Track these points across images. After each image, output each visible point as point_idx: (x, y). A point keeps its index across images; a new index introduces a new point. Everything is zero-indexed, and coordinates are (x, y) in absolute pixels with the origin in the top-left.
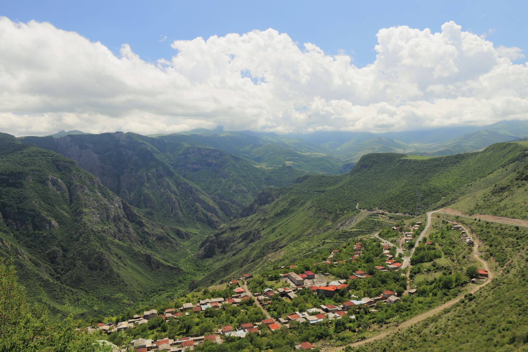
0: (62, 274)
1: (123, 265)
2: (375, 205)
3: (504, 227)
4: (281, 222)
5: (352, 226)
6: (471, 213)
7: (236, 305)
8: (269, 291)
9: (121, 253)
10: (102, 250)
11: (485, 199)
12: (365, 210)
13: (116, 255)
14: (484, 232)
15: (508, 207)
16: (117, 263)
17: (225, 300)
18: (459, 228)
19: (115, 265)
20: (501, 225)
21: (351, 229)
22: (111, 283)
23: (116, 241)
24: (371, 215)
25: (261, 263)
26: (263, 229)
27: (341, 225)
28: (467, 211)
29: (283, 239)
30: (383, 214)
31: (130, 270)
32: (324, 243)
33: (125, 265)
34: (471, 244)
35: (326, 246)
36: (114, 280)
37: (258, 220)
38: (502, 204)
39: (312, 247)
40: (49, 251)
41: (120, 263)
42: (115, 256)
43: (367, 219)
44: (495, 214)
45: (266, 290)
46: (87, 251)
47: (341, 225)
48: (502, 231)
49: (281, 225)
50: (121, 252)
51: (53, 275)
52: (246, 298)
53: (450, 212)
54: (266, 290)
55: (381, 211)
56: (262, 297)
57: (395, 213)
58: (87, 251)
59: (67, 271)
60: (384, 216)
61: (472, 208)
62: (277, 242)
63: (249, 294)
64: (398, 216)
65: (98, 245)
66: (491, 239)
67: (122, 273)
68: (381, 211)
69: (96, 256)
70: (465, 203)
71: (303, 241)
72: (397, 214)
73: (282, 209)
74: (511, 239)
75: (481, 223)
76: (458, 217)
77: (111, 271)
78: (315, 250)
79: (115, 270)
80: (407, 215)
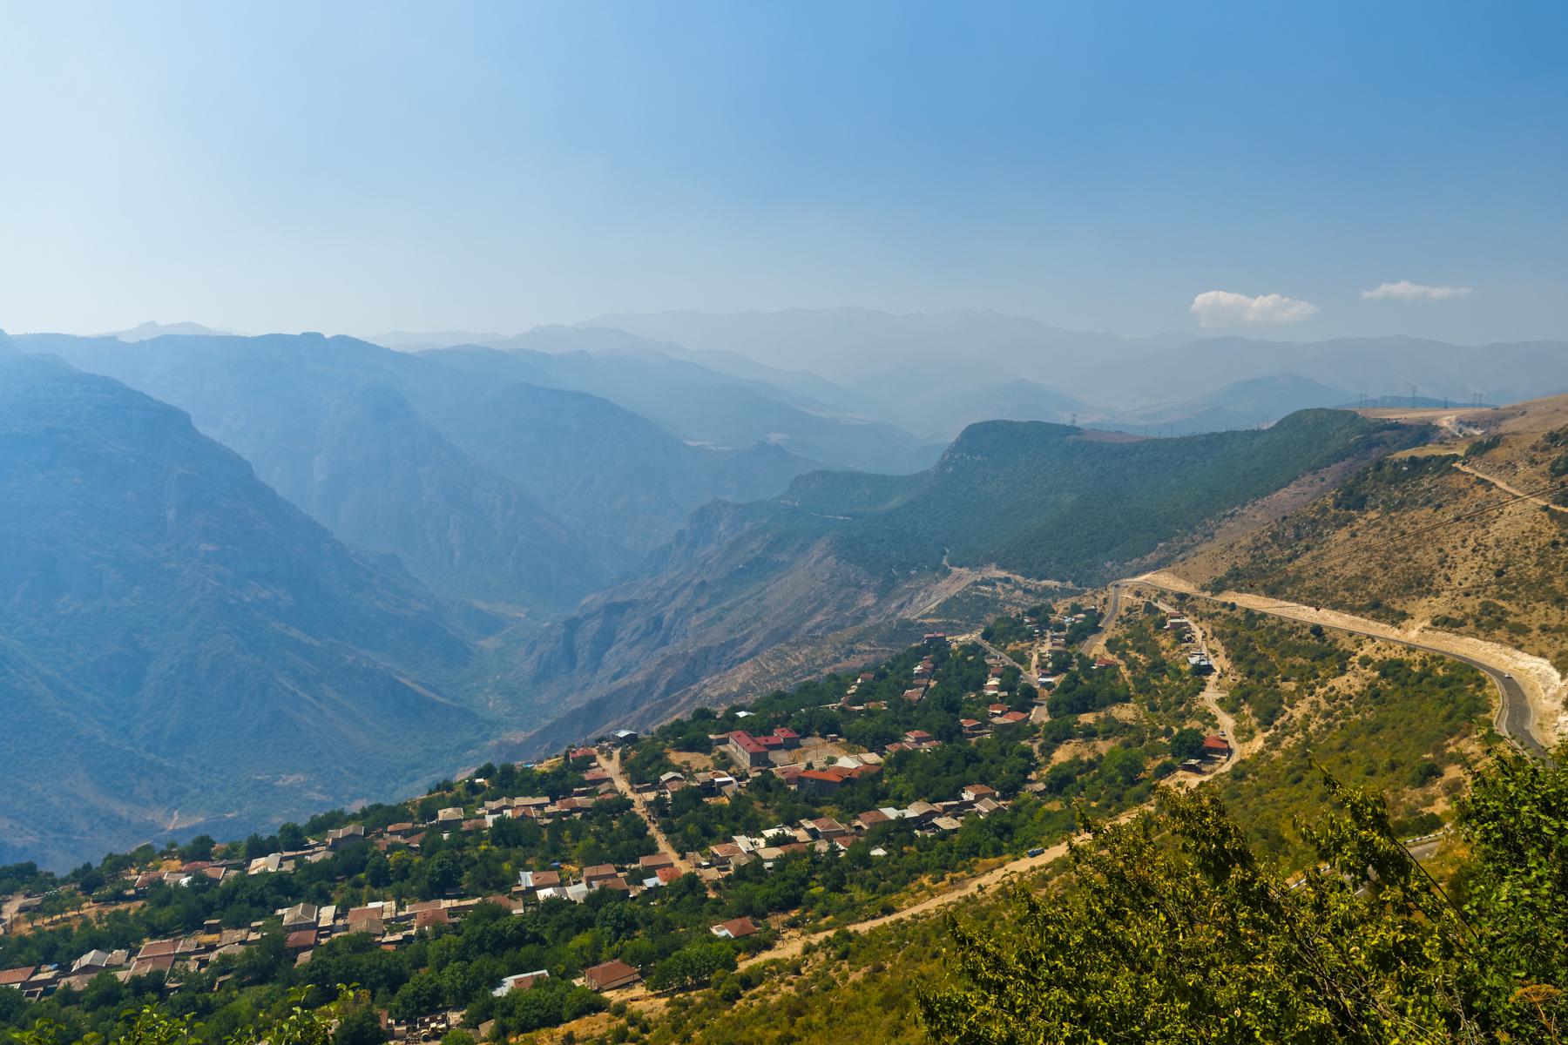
2: (990, 559)
3: (1286, 627)
4: (744, 596)
5: (927, 610)
6: (1218, 587)
7: (579, 815)
8: (674, 778)
11: (1257, 548)
12: (964, 571)
14: (1244, 637)
15: (1305, 575)
17: (553, 802)
18: (1182, 624)
20: (1281, 621)
21: (924, 617)
24: (975, 583)
25: (684, 700)
26: (699, 610)
27: (901, 607)
28: (1208, 581)
29: (746, 638)
30: (1007, 580)
32: (851, 651)
34: (1203, 670)
35: (857, 662)
37: (686, 585)
38: (1290, 568)
39: (819, 662)
43: (965, 594)
44: (1272, 592)
45: (664, 778)
47: (901, 607)
48: (1282, 633)
49: (743, 601)
52: (609, 796)
53: (1164, 580)
54: (664, 778)
55: (1003, 574)
56: (651, 796)
57: (1040, 579)
60: (1008, 587)
61: (1223, 574)
62: (731, 645)
63: (622, 785)
64: (1045, 588)
66: (1252, 656)
68: (1003, 574)
70: (1211, 559)
71: (797, 645)
72: (1045, 582)
73: (750, 557)
74: (1300, 661)
75: (1236, 614)
76: (1182, 597)
78: (826, 671)
80: (1069, 584)
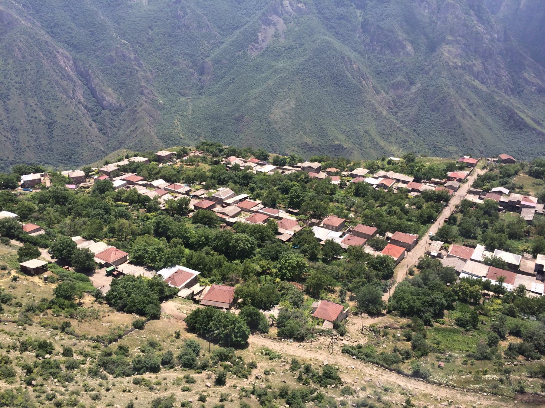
0: (401, 110)
1: (471, 114)
9: (475, 99)
10: (452, 91)
13: (468, 100)
16: (464, 110)
19: (461, 111)
22: (448, 132)
23: (476, 83)
31: (478, 123)
33: (475, 115)
36: (452, 130)
40: (395, 81)
41: (467, 111)
42: (465, 100)
46: (434, 88)
50: (476, 98)
51: (392, 109)
58: (434, 88)
59: (406, 107)
65: (449, 84)
67: (466, 123)
69: (441, 96)
77: (453, 118)
79: (459, 118)
